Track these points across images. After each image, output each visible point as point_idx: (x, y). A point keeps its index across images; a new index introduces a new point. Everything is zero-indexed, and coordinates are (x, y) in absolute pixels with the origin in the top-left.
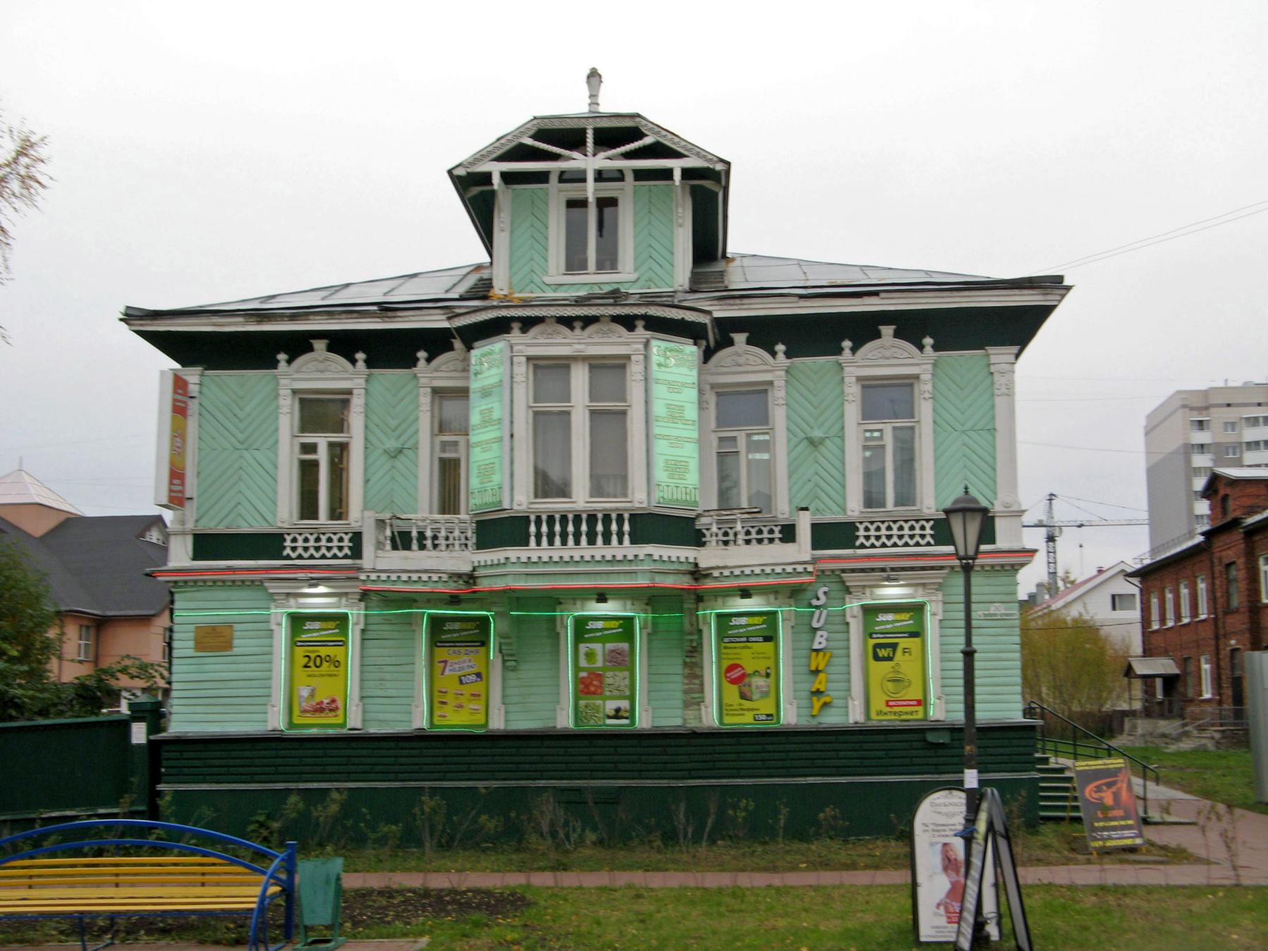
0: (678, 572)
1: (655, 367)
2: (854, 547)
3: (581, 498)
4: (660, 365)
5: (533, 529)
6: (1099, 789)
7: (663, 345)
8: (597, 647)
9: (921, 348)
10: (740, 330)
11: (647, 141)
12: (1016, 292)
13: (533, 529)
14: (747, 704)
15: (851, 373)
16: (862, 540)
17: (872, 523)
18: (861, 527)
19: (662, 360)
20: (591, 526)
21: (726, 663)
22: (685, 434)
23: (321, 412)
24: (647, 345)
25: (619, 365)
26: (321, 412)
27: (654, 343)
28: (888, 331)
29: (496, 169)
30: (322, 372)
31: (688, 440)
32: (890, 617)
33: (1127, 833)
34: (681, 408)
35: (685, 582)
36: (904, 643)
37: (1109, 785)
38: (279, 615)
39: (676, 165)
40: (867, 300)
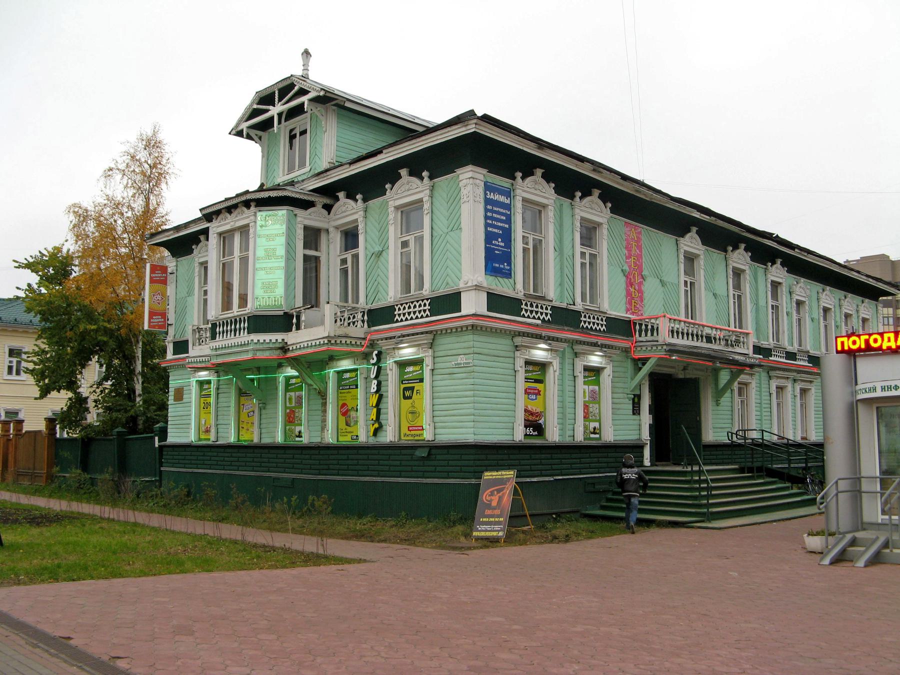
0: (271, 349)
1: (258, 228)
4: (262, 226)
6: (492, 494)
7: (264, 214)
8: (293, 394)
9: (422, 179)
11: (296, 88)
12: (449, 129)
14: (349, 429)
16: (397, 317)
17: (402, 305)
18: (397, 308)
19: (263, 223)
21: (341, 403)
22: (276, 265)
24: (255, 215)
25: (244, 230)
27: (259, 214)
28: (404, 172)
31: (278, 268)
32: (410, 369)
33: (497, 527)
34: (274, 250)
35: (276, 354)
36: (417, 386)
37: (499, 491)
38: (193, 381)
39: (305, 99)
40: (379, 157)
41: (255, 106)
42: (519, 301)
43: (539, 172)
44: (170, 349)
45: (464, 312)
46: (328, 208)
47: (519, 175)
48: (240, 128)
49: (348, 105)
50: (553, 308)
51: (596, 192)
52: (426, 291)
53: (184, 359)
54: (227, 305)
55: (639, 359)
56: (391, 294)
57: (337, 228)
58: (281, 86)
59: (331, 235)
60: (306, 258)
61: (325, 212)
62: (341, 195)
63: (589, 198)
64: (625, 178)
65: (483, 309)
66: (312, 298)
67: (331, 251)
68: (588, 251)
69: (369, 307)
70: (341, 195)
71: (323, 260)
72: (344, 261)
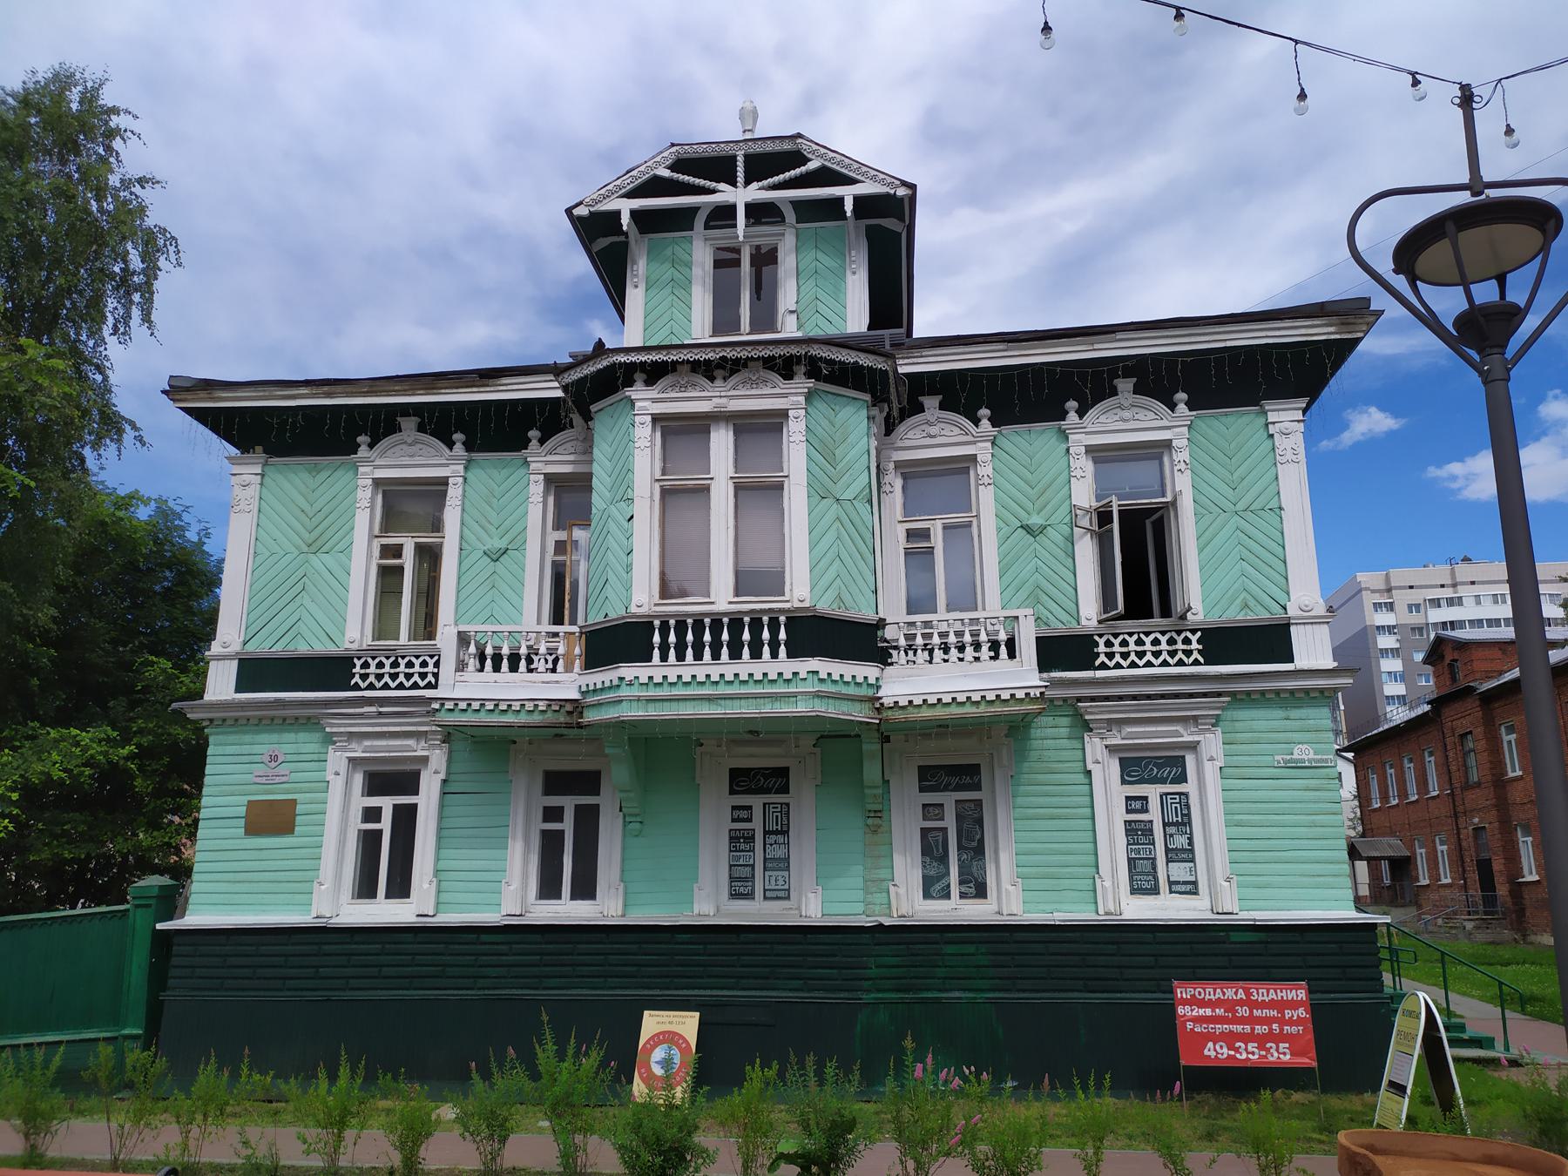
2: (1091, 667)
3: (722, 597)
5: (657, 638)
9: (1172, 406)
10: (931, 393)
11: (813, 165)
13: (657, 638)
15: (1078, 441)
16: (1102, 658)
20: (734, 634)
23: (409, 505)
26: (409, 505)
29: (626, 207)
30: (412, 459)
39: (847, 193)
41: (666, 173)
58: (758, 148)
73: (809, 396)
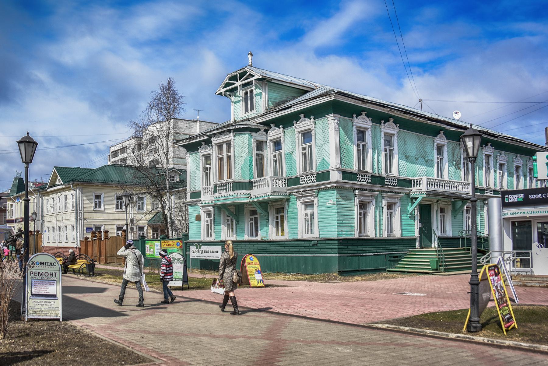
9: (311, 119)
11: (248, 74)
28: (302, 116)
29: (223, 91)
39: (252, 79)
41: (228, 81)
42: (356, 174)
43: (364, 113)
44: (188, 196)
45: (331, 181)
46: (266, 131)
47: (355, 116)
48: (220, 92)
49: (273, 81)
50: (372, 176)
51: (392, 120)
52: (314, 171)
53: (198, 201)
54: (221, 177)
55: (414, 198)
56: (299, 170)
57: (271, 140)
59: (268, 144)
60: (258, 155)
61: (265, 133)
62: (272, 125)
63: (388, 123)
64: (406, 112)
65: (340, 179)
66: (261, 174)
67: (269, 152)
68: (388, 148)
69: (287, 177)
70: (272, 125)
71: (265, 156)
72: (275, 156)
73: (235, 136)
